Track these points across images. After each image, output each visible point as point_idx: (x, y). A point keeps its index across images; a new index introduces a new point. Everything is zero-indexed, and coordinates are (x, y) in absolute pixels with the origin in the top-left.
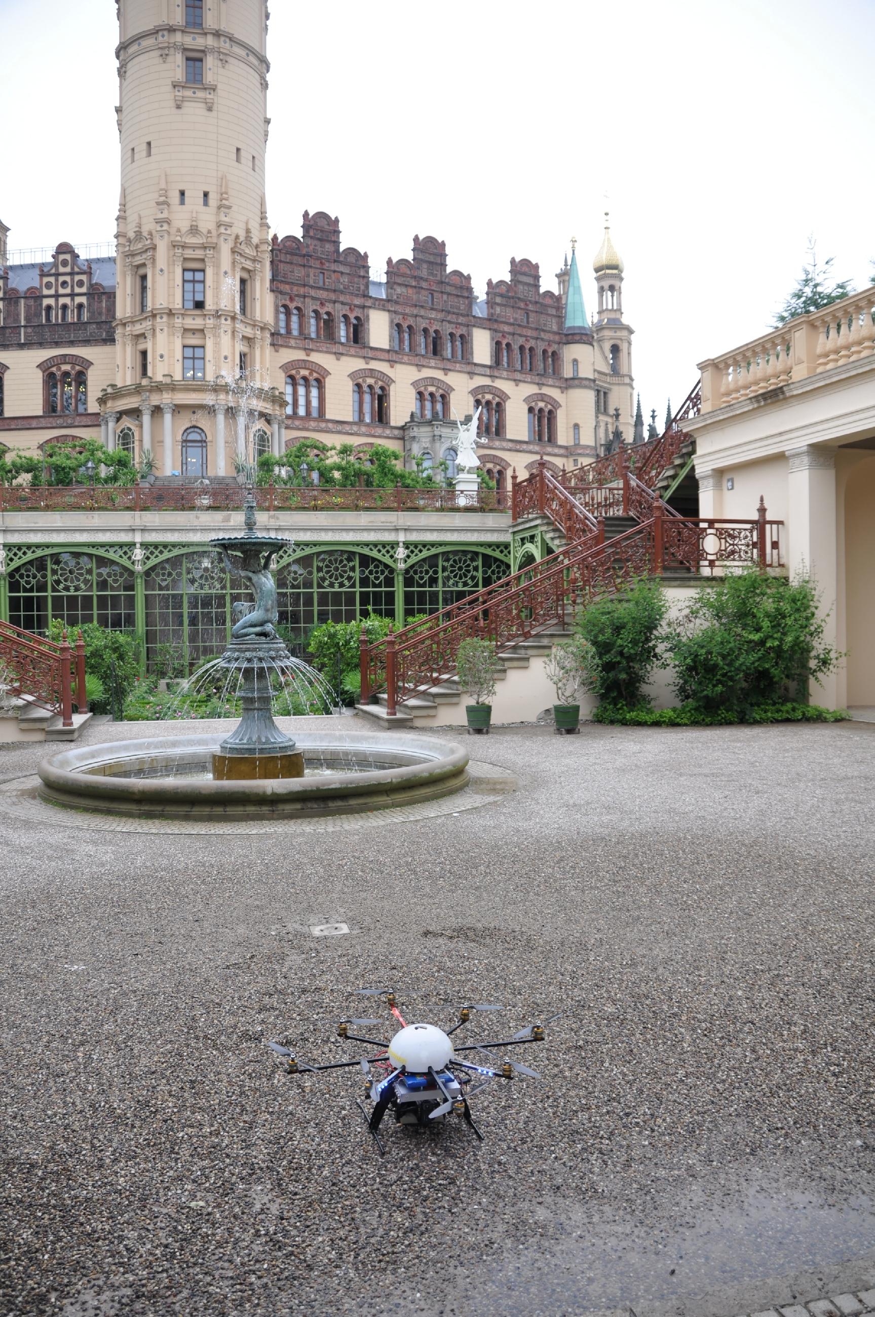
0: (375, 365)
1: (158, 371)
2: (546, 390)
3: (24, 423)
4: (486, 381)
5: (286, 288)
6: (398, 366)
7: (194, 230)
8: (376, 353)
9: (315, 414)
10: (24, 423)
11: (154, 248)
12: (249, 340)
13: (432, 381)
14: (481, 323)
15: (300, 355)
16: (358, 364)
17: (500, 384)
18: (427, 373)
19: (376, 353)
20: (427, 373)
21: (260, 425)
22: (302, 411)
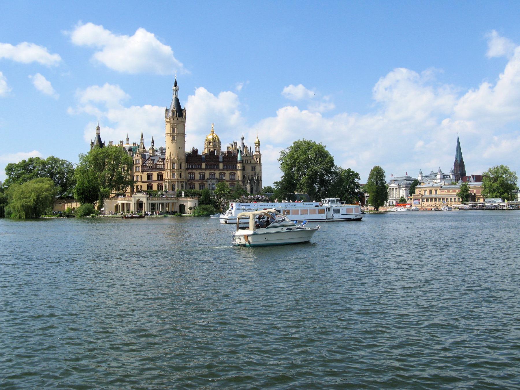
0: (203, 171)
1: (169, 177)
2: (233, 171)
3: (155, 181)
4: (222, 171)
5: (189, 162)
6: (207, 171)
7: (174, 159)
8: (203, 169)
9: (193, 179)
10: (155, 181)
11: (169, 161)
12: (181, 172)
13: (212, 172)
14: (221, 162)
15: (191, 171)
16: (200, 171)
17: (224, 171)
18: (211, 171)
19: (203, 169)
20: (211, 171)
21: (182, 183)
22: (191, 179)
